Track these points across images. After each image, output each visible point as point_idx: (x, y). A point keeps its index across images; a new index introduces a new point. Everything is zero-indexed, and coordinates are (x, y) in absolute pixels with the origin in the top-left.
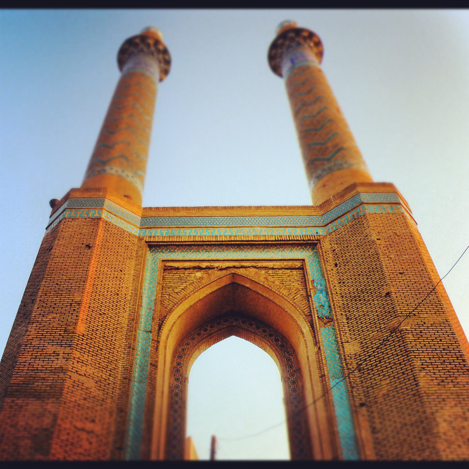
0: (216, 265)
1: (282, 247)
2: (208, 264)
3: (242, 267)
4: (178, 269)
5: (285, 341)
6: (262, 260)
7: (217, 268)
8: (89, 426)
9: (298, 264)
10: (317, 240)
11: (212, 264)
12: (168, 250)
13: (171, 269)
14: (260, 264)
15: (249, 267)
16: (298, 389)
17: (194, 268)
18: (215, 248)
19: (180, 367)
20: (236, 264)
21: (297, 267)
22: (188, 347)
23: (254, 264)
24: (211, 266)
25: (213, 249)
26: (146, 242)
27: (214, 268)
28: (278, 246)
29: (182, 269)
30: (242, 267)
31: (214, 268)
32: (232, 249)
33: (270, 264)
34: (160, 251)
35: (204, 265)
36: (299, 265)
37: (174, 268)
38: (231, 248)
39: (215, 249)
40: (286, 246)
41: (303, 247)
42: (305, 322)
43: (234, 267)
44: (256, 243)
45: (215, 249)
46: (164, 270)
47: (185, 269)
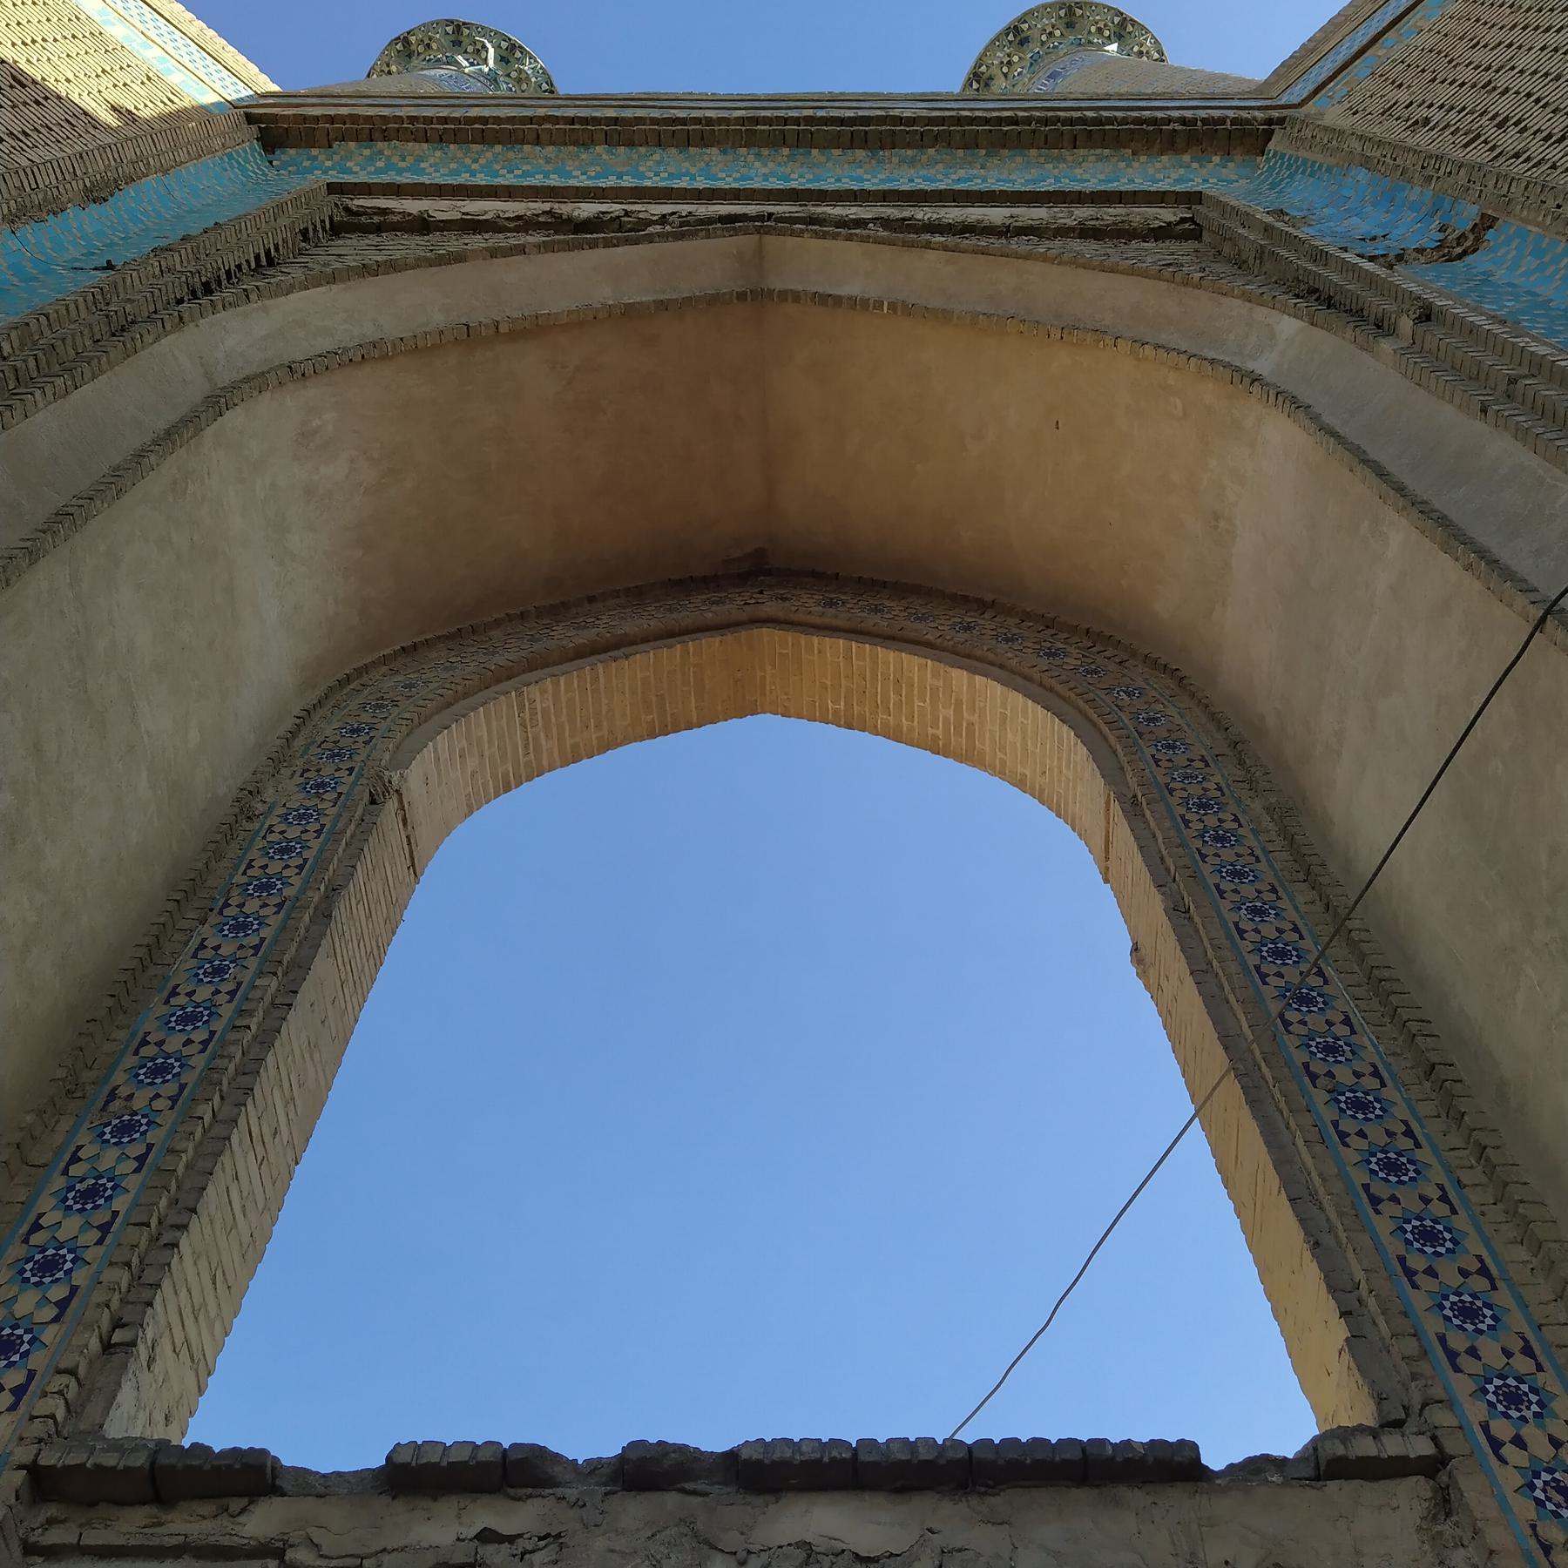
2: (616, 208)
4: (423, 225)
7: (663, 219)
9: (1168, 215)
11: (629, 208)
12: (380, 164)
13: (378, 229)
14: (923, 214)
16: (1255, 832)
18: (657, 157)
21: (1157, 224)
23: (893, 212)
24: (627, 213)
25: (649, 163)
28: (1033, 152)
32: (757, 164)
34: (329, 164)
35: (587, 210)
36: (1173, 219)
37: (396, 218)
38: (751, 158)
39: (658, 163)
40: (1082, 152)
41: (1186, 158)
42: (1261, 313)
45: (658, 163)
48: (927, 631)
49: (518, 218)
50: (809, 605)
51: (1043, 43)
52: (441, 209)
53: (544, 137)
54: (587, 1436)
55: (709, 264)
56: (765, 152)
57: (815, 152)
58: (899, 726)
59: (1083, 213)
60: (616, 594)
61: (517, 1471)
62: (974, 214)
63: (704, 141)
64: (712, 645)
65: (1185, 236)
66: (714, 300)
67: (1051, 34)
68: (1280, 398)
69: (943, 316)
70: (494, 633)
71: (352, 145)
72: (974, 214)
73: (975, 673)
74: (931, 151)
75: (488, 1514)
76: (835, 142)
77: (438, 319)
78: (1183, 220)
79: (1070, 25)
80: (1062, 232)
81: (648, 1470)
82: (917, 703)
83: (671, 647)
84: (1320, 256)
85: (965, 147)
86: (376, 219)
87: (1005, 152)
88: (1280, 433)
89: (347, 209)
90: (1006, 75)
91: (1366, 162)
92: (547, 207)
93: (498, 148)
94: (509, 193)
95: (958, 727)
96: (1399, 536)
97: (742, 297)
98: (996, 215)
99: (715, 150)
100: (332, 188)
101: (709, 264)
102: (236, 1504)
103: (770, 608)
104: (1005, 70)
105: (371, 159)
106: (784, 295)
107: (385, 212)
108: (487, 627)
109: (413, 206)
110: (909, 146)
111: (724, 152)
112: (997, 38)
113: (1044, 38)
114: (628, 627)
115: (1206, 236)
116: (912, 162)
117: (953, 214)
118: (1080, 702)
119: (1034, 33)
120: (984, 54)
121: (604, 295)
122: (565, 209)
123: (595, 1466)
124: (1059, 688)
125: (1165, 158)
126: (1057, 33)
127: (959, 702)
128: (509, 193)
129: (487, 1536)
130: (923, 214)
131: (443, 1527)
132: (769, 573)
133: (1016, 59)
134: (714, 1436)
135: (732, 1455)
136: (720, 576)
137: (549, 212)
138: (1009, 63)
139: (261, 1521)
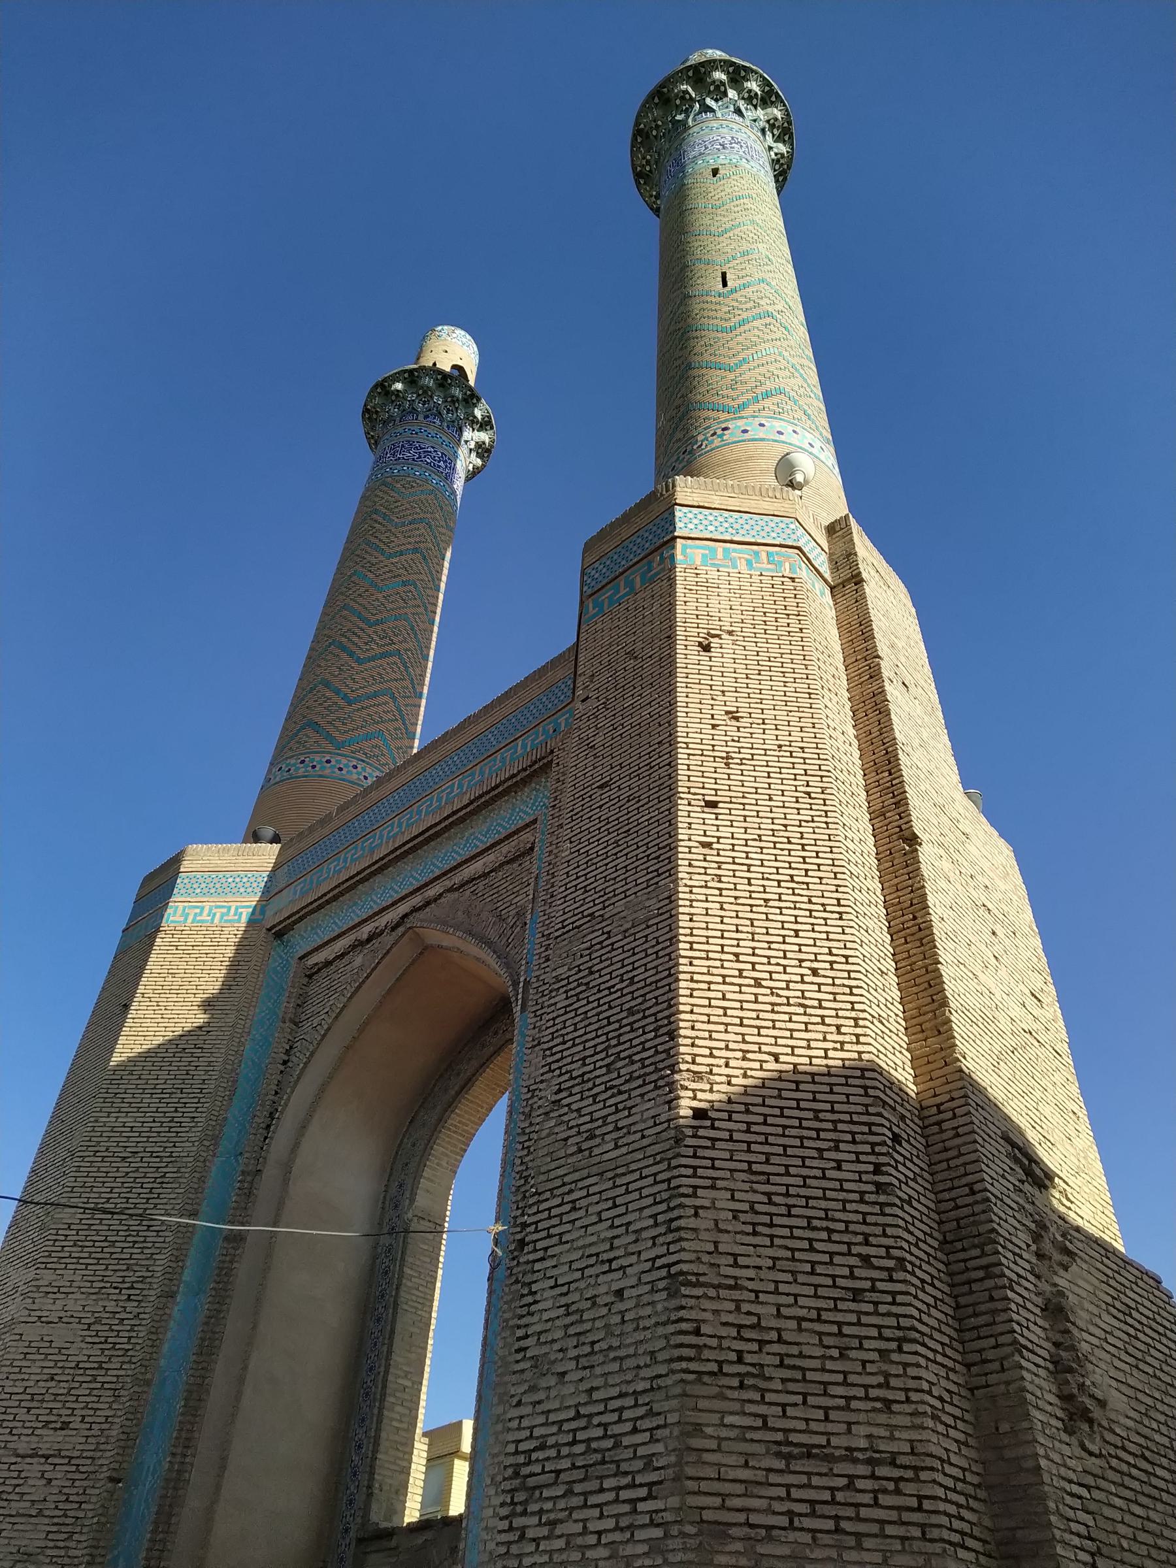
0: (382, 921)
1: (494, 809)
3: (428, 903)
4: (328, 963)
8: (50, 1440)
11: (376, 924)
13: (319, 970)
14: (457, 879)
20: (417, 900)
23: (448, 884)
26: (269, 930)
27: (382, 932)
29: (334, 959)
30: (428, 903)
31: (382, 932)
33: (477, 867)
43: (415, 910)
44: (439, 828)
59: (505, 849)
92: (353, 937)
97: (421, 953)
98: (477, 867)
107: (317, 964)
116: (449, 839)
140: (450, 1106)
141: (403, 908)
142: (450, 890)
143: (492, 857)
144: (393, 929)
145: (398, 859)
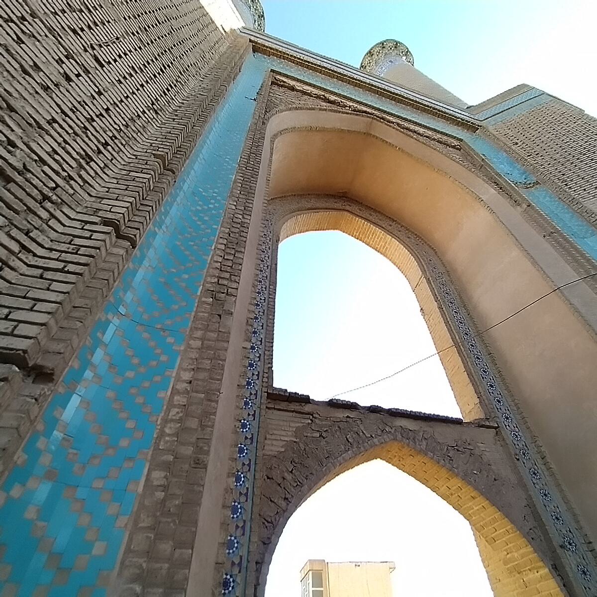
1: (434, 119)
4: (293, 89)
5: (420, 240)
6: (410, 121)
7: (350, 107)
9: (456, 143)
10: (478, 126)
13: (282, 86)
15: (393, 123)
17: (318, 97)
18: (347, 87)
19: (270, 223)
22: (282, 208)
24: (341, 102)
26: (251, 41)
28: (430, 115)
34: (269, 61)
35: (333, 98)
40: (439, 119)
41: (460, 128)
43: (372, 114)
46: (273, 83)
47: (304, 93)
48: (380, 223)
49: (316, 94)
50: (355, 208)
51: (389, 50)
52: (298, 86)
53: (323, 72)
54: (364, 402)
55: (359, 123)
56: (373, 94)
57: (384, 98)
58: (369, 243)
59: (439, 136)
60: (314, 194)
61: (353, 406)
62: (417, 128)
63: (360, 86)
64: (335, 213)
65: (457, 149)
66: (359, 132)
67: (391, 49)
68: (489, 208)
69: (410, 155)
70: (289, 198)
71: (275, 57)
72: (417, 128)
73: (393, 237)
74: (409, 107)
75: (347, 413)
76: (388, 97)
77: (306, 124)
78: (458, 145)
79: (395, 47)
80: (434, 139)
81: (375, 410)
82: (376, 239)
83: (327, 212)
84: (497, 174)
85: (415, 108)
86: (282, 83)
87: (424, 113)
88: (484, 213)
89: (275, 78)
90: (377, 55)
91: (506, 151)
92: (323, 94)
93: (311, 71)
94: (314, 86)
95: (384, 247)
96: (516, 253)
98: (421, 130)
99: (361, 90)
100: (272, 71)
101: (359, 123)
102: (303, 404)
103: (348, 208)
104: (378, 54)
105: (279, 63)
106: (374, 136)
107: (284, 82)
108: (288, 196)
109: (292, 83)
110: (404, 104)
111: (363, 91)
112: (378, 44)
113: (389, 49)
114: (318, 205)
115: (462, 150)
116: (404, 109)
117: (412, 127)
118: (416, 253)
119: (387, 47)
120: (373, 47)
121: (338, 125)
122: (327, 96)
123: (365, 407)
124: (411, 247)
125: (456, 127)
126: (393, 49)
127: (386, 242)
128: (314, 86)
129: (348, 417)
130: (406, 125)
131: (341, 414)
132: (346, 198)
133: (381, 52)
134: (386, 406)
135: (390, 410)
136: (337, 196)
137: (324, 96)
138: (379, 52)
139: (307, 408)
140: (300, 210)
141: (365, 109)
142: (398, 124)
143: (430, 133)
144: (354, 111)
145: (370, 90)
